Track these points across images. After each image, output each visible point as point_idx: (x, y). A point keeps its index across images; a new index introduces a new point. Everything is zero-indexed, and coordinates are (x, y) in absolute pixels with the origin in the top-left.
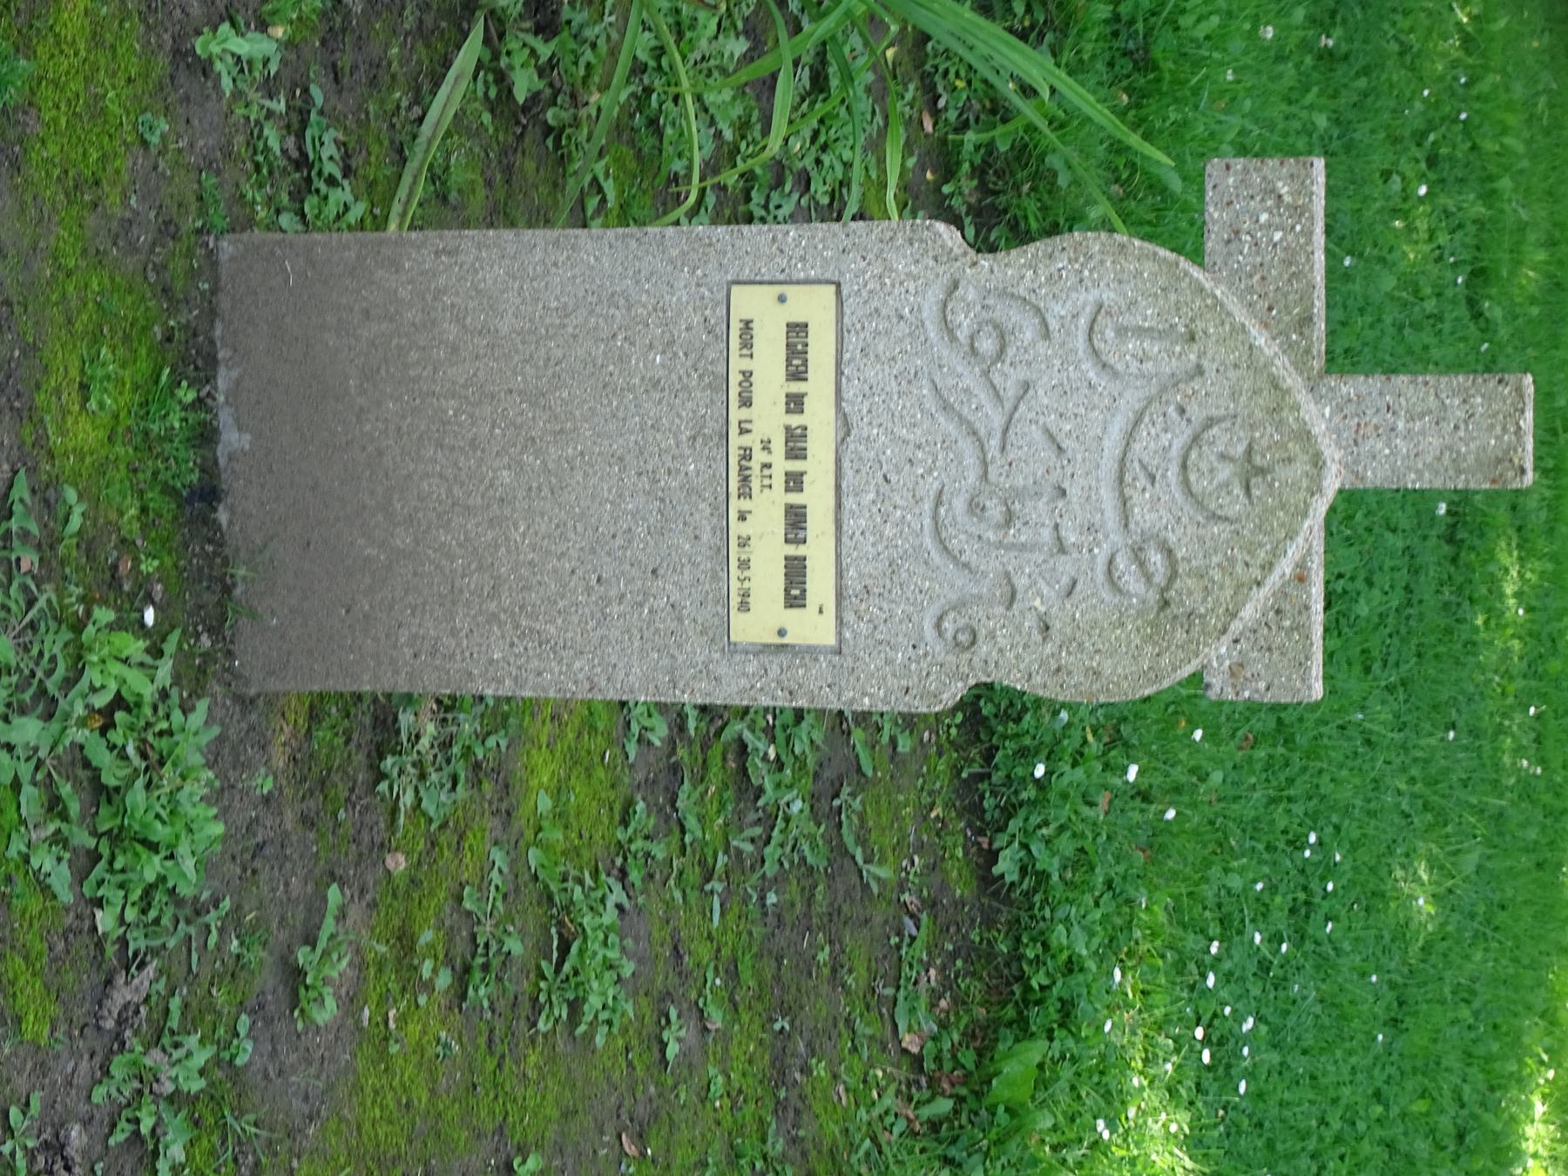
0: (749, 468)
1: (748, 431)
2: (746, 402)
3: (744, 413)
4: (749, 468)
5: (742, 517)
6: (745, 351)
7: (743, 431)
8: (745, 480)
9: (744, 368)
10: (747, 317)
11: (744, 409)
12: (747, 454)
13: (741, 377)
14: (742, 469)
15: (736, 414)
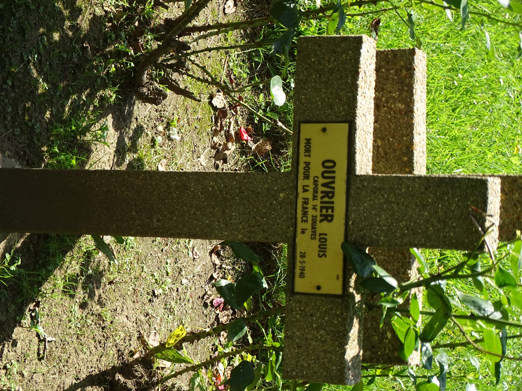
0: (307, 208)
1: (308, 191)
2: (307, 177)
3: (306, 182)
4: (307, 208)
5: (303, 232)
6: (307, 154)
7: (305, 191)
8: (305, 214)
9: (307, 161)
10: (308, 137)
11: (306, 180)
12: (306, 201)
13: (304, 165)
14: (304, 208)
15: (301, 183)
